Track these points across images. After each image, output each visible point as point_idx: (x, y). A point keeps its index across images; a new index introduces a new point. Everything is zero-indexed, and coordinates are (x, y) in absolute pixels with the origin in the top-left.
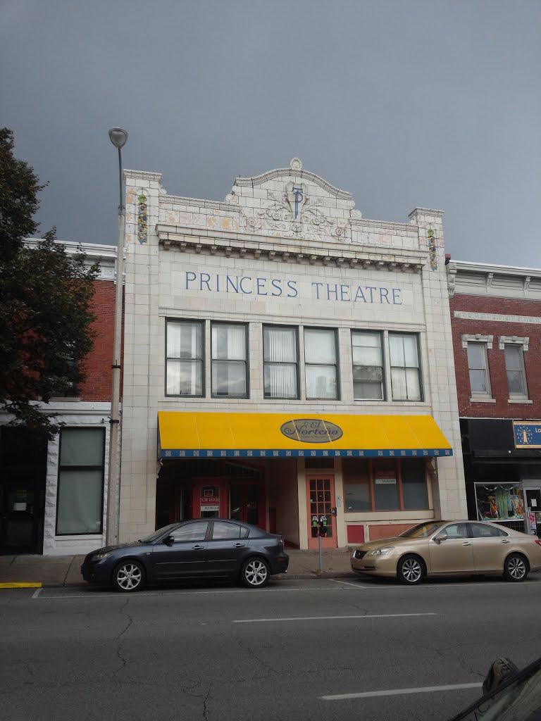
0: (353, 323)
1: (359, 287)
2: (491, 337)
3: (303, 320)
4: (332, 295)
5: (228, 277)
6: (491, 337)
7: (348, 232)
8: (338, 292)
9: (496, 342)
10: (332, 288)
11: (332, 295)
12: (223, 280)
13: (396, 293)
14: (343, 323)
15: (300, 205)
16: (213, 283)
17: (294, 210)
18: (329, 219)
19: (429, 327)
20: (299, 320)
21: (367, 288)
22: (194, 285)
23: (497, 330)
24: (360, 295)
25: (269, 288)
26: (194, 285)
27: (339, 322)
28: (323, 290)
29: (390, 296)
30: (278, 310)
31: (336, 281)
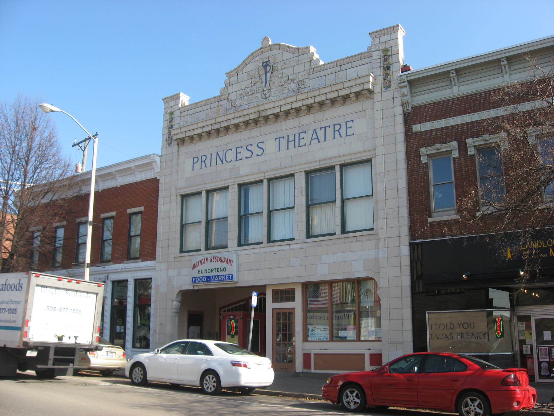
0: (306, 166)
1: (315, 130)
2: (454, 144)
3: (266, 174)
4: (291, 144)
5: (217, 154)
6: (454, 144)
7: (307, 82)
8: (295, 141)
9: (463, 148)
10: (291, 138)
11: (291, 144)
12: (214, 156)
13: (349, 125)
14: (297, 168)
15: (269, 75)
16: (208, 162)
17: (264, 80)
18: (291, 77)
19: (380, 151)
20: (263, 175)
21: (321, 128)
22: (197, 166)
23: (459, 134)
24: (315, 136)
25: (245, 153)
26: (197, 166)
27: (294, 168)
28: (284, 142)
29: (343, 131)
30: (247, 171)
31: (296, 131)
